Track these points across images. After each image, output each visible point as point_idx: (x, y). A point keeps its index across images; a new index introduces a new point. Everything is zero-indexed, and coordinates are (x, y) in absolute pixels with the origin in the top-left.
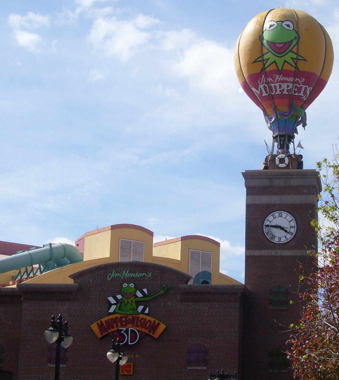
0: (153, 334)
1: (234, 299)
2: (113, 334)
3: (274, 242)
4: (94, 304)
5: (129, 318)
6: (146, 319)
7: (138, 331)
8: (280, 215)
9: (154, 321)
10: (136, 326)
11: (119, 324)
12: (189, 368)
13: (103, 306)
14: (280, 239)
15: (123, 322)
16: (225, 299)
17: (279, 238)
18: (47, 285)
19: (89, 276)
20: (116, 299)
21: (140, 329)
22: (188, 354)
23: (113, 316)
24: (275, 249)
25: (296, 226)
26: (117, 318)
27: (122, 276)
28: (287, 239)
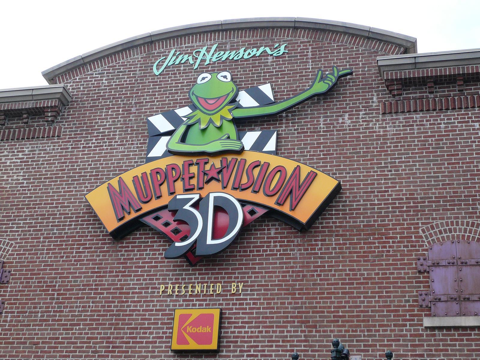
0: (293, 209)
2: (157, 218)
4: (106, 140)
5: (213, 165)
6: (269, 165)
7: (243, 203)
9: (295, 169)
10: (235, 189)
11: (179, 185)
12: (427, 322)
13: (132, 144)
15: (191, 178)
19: (100, 69)
20: (175, 120)
21: (248, 195)
22: (420, 272)
23: (162, 164)
26: (173, 167)
27: (195, 62)
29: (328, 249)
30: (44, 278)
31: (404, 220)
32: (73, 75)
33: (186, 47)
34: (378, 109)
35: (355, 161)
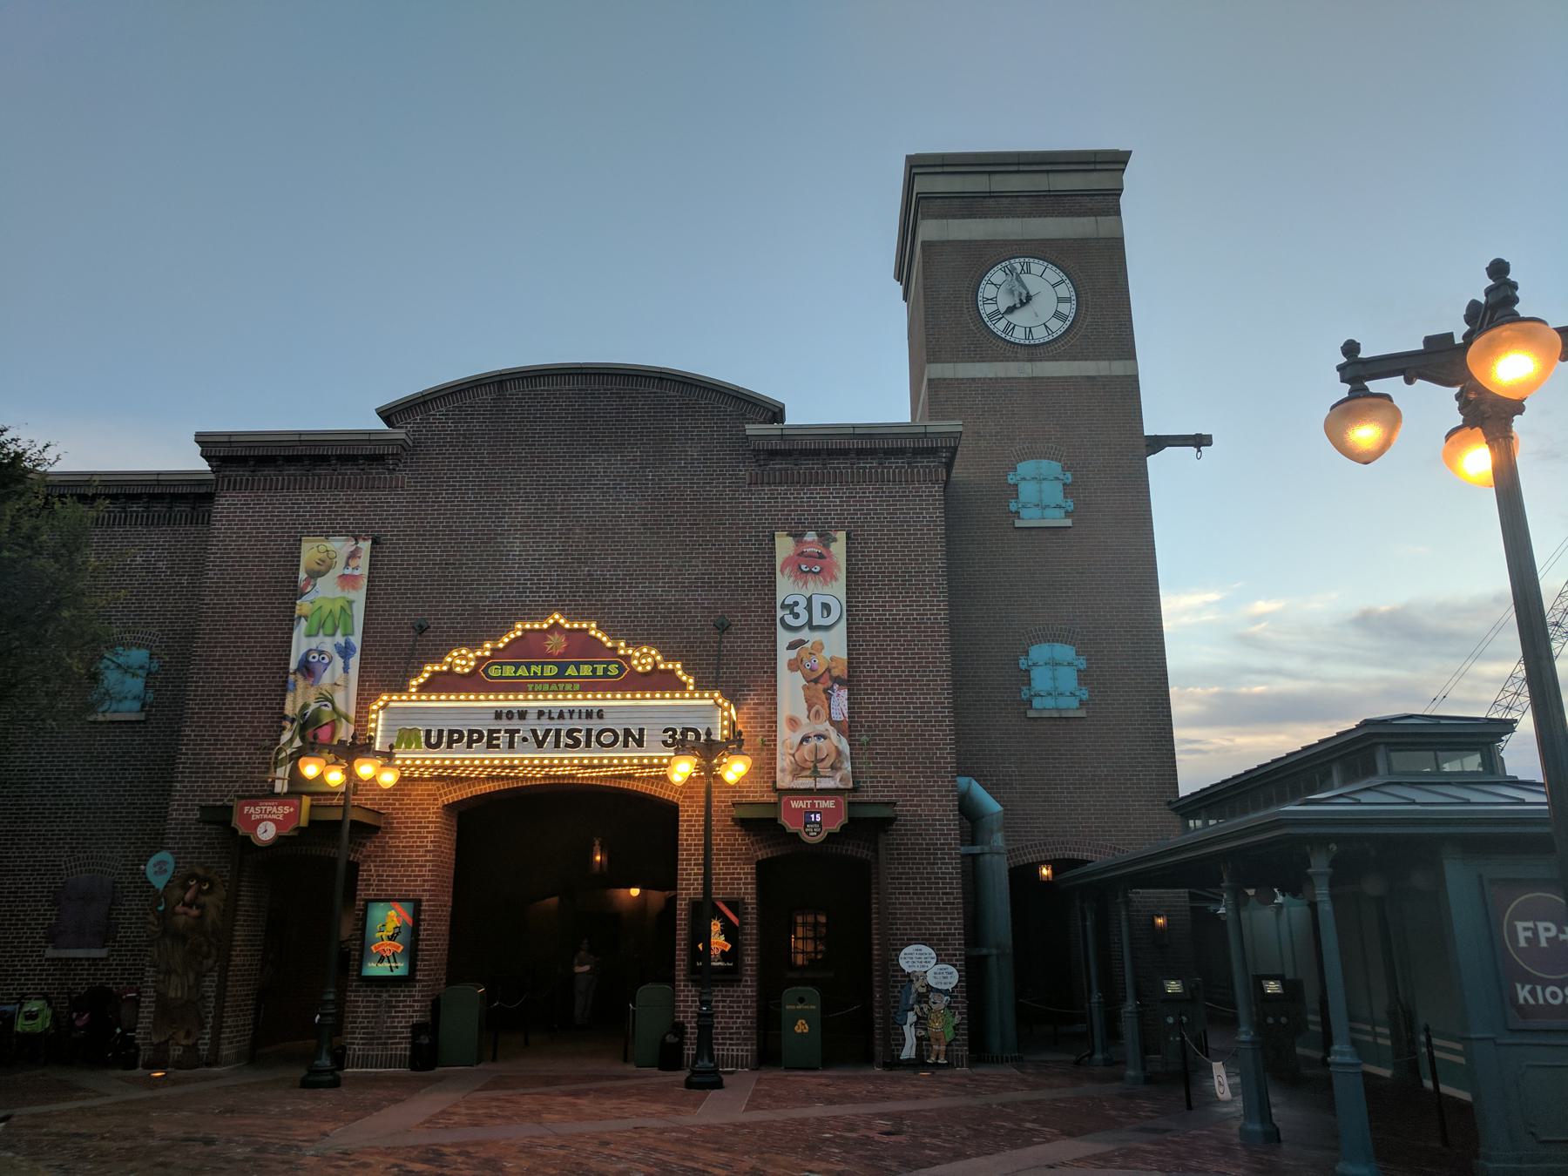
1: (925, 471)
3: (1012, 340)
8: (1025, 268)
14: (1030, 331)
16: (894, 472)
17: (1028, 330)
18: (300, 433)
24: (1016, 359)
25: (1074, 298)
28: (1050, 333)
29: (694, 621)
30: (401, 645)
31: (765, 594)
32: (413, 414)
33: (542, 390)
34: (745, 478)
35: (721, 532)
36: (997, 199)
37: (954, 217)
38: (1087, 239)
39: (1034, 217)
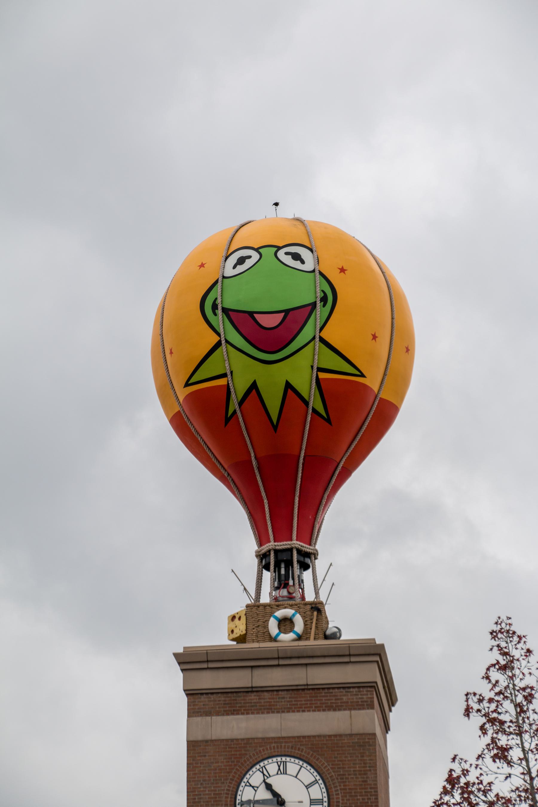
36: (258, 694)
37: (218, 714)
38: (340, 736)
39: (294, 711)
